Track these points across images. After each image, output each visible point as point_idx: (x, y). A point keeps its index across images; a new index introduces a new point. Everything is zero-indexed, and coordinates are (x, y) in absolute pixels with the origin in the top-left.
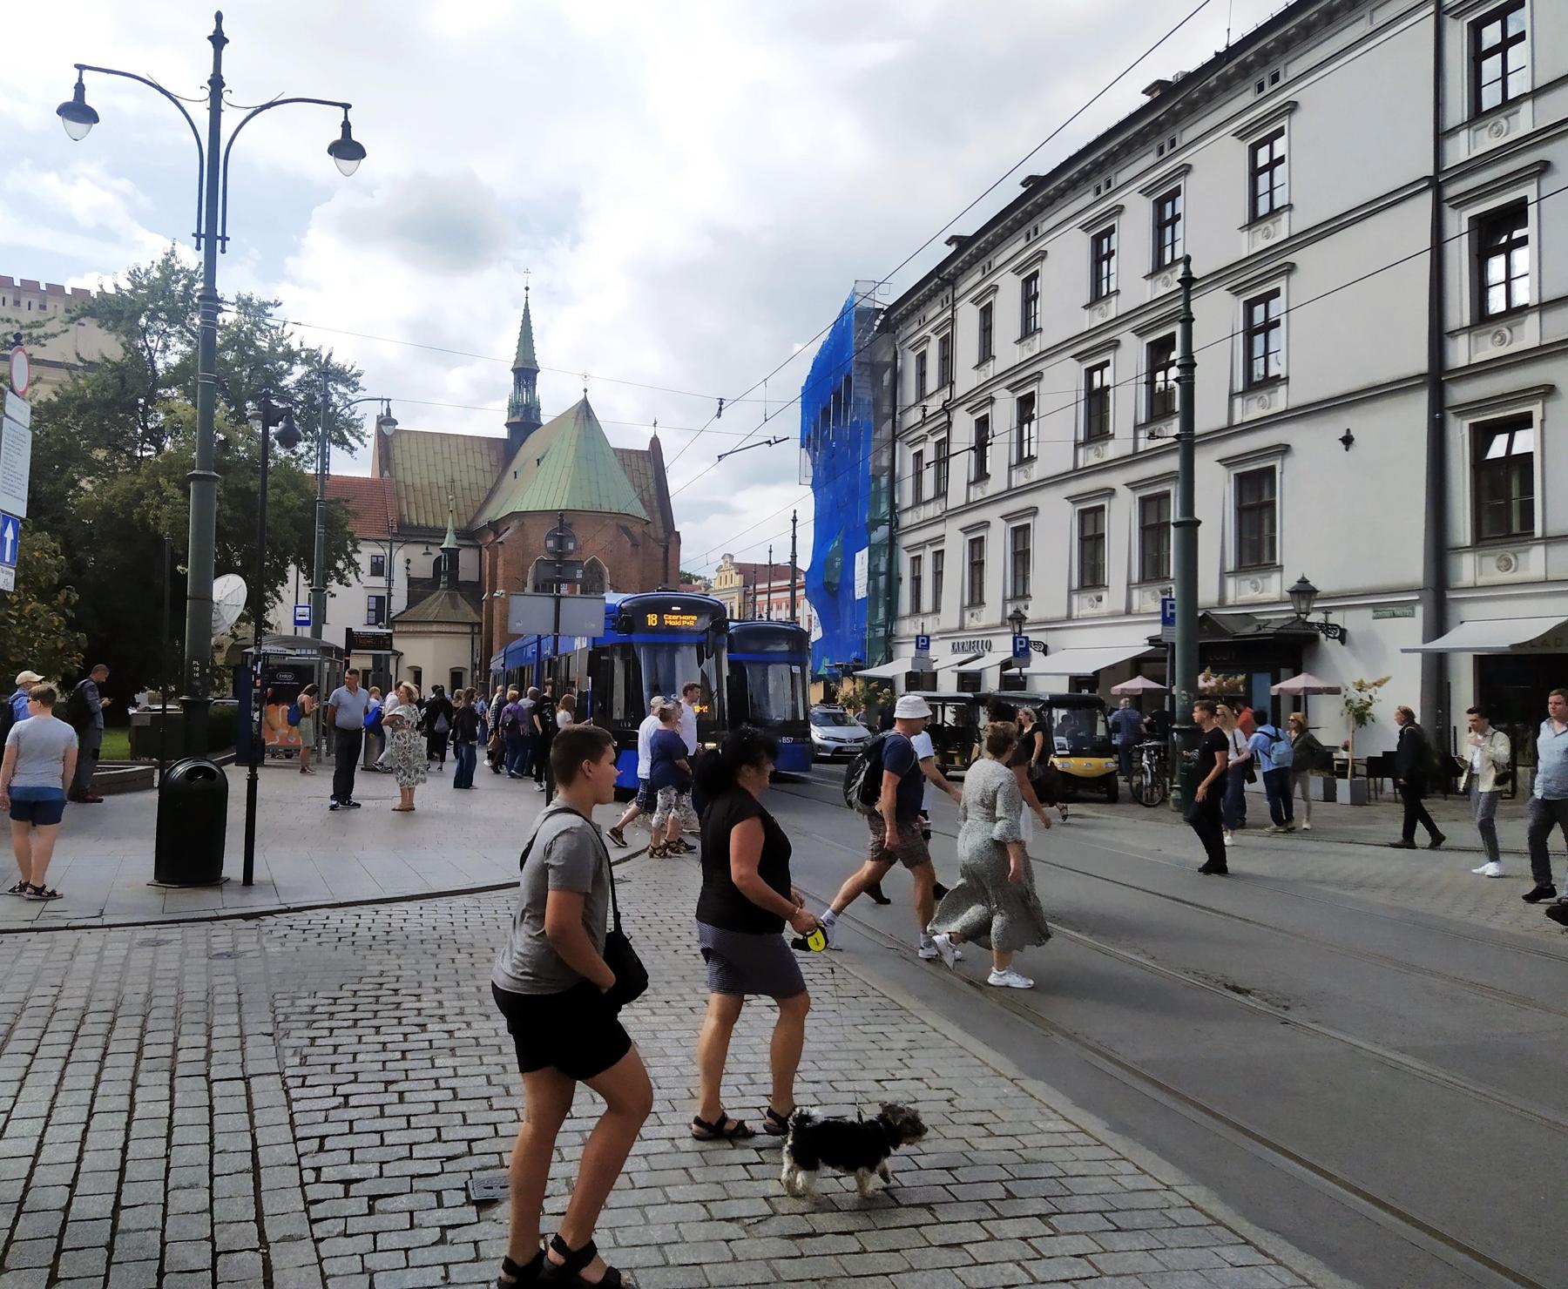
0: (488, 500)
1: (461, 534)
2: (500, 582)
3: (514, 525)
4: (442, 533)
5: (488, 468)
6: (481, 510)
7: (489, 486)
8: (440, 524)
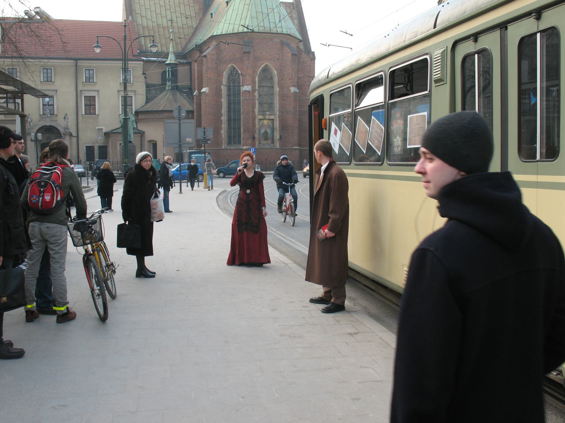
0: (194, 34)
1: (178, 56)
2: (205, 81)
3: (214, 43)
4: (166, 56)
5: (193, 14)
6: (190, 41)
7: (195, 26)
8: (165, 50)
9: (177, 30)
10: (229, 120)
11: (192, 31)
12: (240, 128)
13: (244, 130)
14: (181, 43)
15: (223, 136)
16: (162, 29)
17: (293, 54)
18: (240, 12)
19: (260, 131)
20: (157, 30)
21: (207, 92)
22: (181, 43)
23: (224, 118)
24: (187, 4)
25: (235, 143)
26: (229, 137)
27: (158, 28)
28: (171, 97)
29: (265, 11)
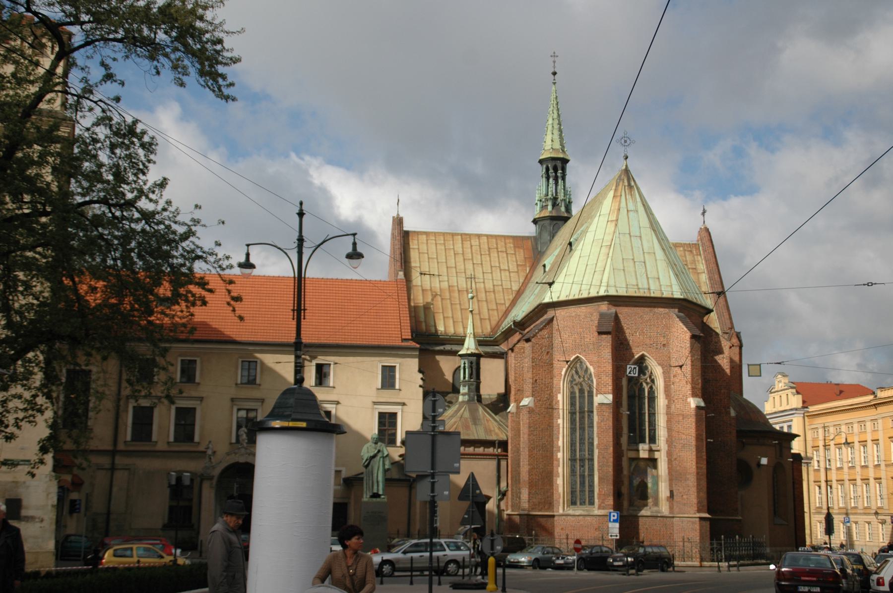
0: (514, 303)
4: (461, 342)
5: (513, 267)
7: (515, 287)
8: (460, 331)
9: (483, 295)
10: (572, 460)
11: (511, 297)
12: (591, 475)
13: (600, 478)
14: (489, 319)
15: (561, 490)
16: (456, 294)
17: (693, 337)
18: (592, 261)
19: (631, 483)
20: (447, 295)
21: (532, 405)
22: (489, 319)
23: (561, 455)
24: (504, 249)
25: (583, 503)
26: (573, 492)
27: (450, 292)
28: (467, 415)
29: (639, 257)
